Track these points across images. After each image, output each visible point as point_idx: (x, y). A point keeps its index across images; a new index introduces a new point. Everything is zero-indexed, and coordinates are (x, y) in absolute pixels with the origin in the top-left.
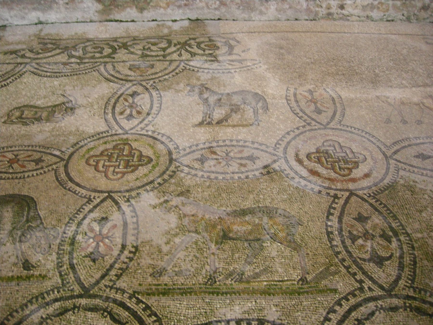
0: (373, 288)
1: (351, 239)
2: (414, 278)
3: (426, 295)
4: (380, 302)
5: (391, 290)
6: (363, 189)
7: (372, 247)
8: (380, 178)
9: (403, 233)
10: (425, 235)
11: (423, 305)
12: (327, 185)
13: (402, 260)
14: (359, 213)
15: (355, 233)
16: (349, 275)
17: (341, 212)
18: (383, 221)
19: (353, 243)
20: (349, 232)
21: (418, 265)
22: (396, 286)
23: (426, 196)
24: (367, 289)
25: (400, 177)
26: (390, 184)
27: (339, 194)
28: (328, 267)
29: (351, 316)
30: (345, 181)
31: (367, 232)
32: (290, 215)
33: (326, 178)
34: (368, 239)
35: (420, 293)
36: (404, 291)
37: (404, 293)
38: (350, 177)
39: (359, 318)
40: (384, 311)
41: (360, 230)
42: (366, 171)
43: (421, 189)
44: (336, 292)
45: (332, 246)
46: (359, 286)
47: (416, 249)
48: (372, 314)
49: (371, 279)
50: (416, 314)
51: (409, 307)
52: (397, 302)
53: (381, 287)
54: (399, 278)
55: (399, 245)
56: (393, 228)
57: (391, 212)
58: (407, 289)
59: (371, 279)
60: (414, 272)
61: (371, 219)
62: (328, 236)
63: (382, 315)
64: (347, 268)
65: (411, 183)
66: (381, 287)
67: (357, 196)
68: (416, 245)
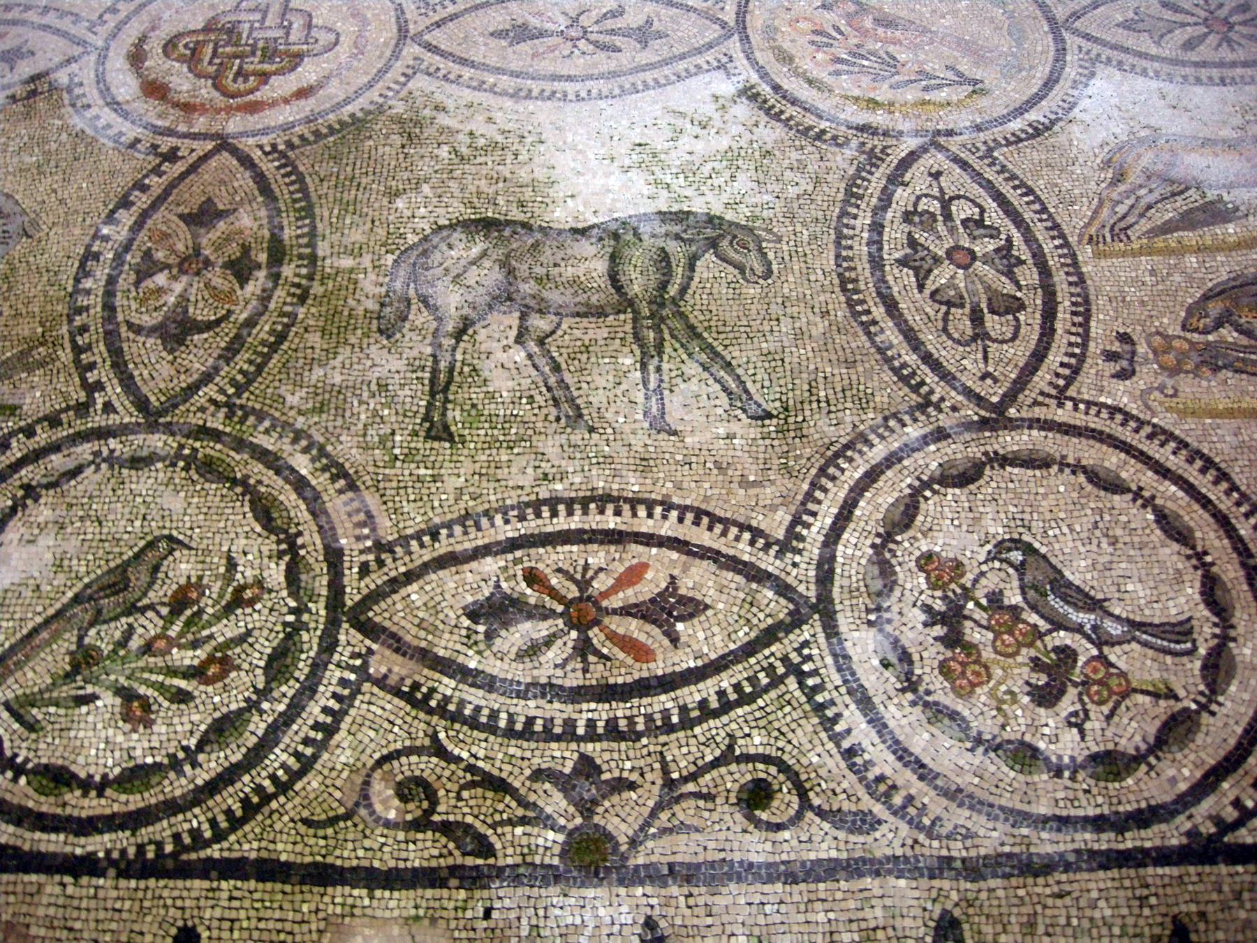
0: (117, 404)
1: (138, 272)
2: (250, 382)
3: (255, 427)
4: (112, 443)
5: (160, 414)
6: (265, 131)
7: (183, 298)
8: (342, 96)
9: (300, 257)
10: (366, 261)
11: (232, 453)
12: (167, 124)
13: (245, 332)
14: (209, 200)
15: (160, 255)
16: (73, 370)
17: (158, 197)
18: (265, 221)
19: (137, 284)
20: (148, 254)
21: (285, 346)
22: (185, 401)
23: (444, 152)
24: (99, 406)
25: (403, 94)
26: (360, 115)
27: (184, 145)
28: (31, 349)
29: (16, 476)
30: (239, 108)
31: (197, 251)
32: (17, 209)
33: (176, 105)
34: (186, 273)
35: (242, 421)
36: (199, 415)
37: (196, 420)
38: (251, 97)
39: (34, 483)
40: (111, 467)
41: (180, 247)
42: (312, 78)
43: (442, 130)
44: (13, 414)
45: (76, 291)
46: (83, 399)
47: (310, 301)
48: (75, 472)
49: (127, 382)
50: (195, 477)
51: (185, 458)
52: (160, 444)
53: (142, 404)
54: (207, 378)
55: (264, 290)
56: (281, 241)
57: (307, 196)
58: (212, 408)
59: (127, 382)
60: (260, 369)
61: (232, 218)
62: (82, 265)
63: (98, 477)
64: (78, 350)
65: (427, 112)
66: (142, 404)
67: (234, 151)
68: (317, 289)
